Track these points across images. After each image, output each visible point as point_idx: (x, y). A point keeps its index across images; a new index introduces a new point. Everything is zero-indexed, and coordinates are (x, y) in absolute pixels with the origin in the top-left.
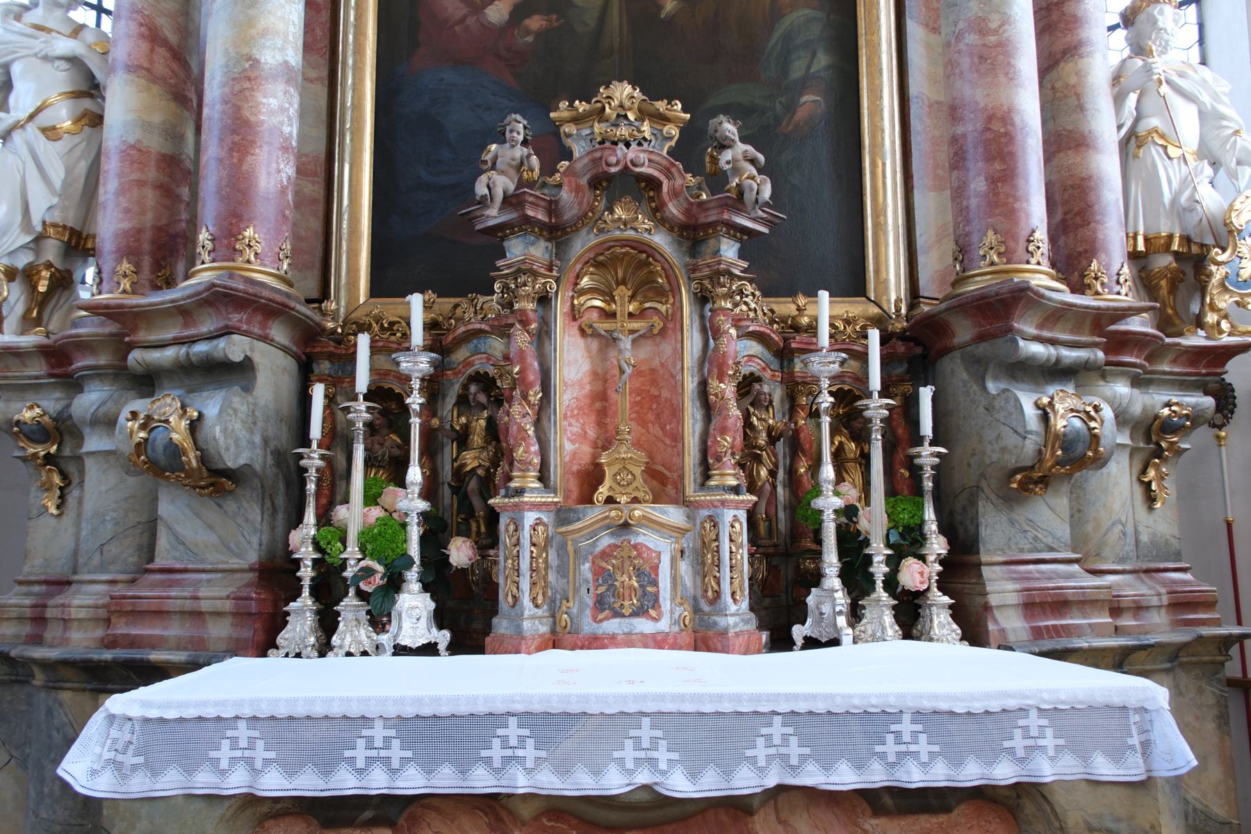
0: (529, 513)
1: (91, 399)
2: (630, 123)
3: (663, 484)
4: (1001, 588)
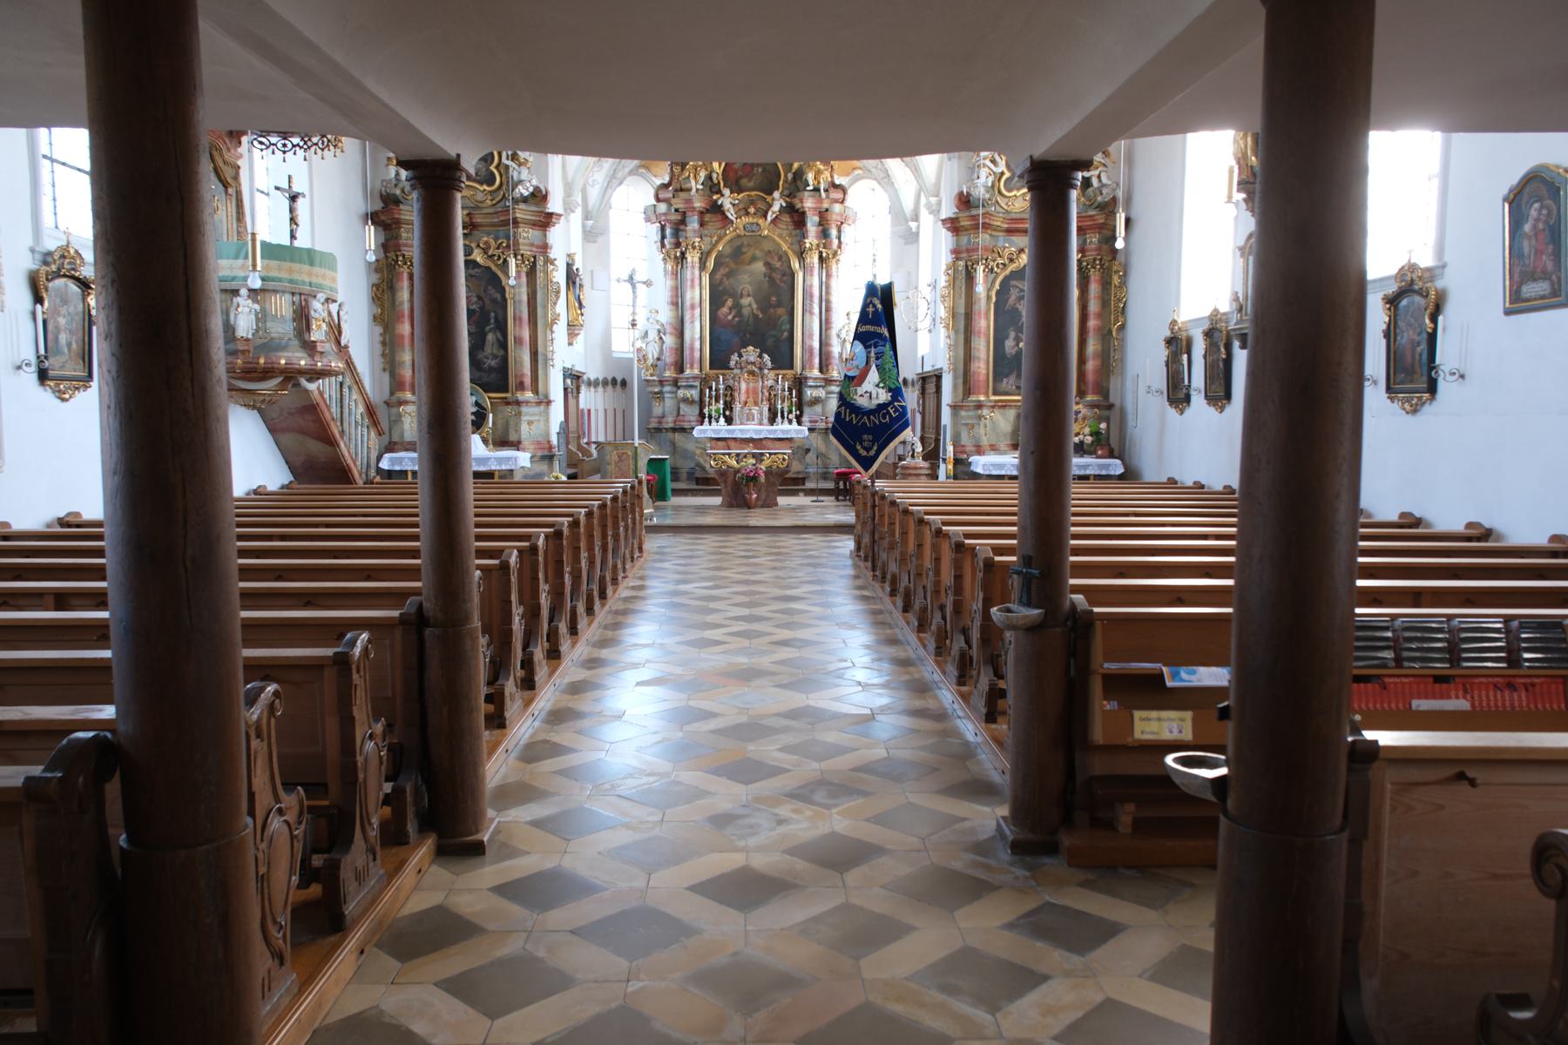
0: (737, 407)
1: (667, 389)
2: (751, 353)
3: (756, 404)
4: (805, 419)
